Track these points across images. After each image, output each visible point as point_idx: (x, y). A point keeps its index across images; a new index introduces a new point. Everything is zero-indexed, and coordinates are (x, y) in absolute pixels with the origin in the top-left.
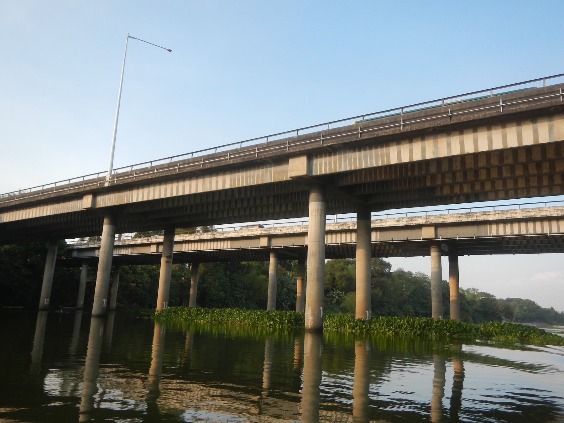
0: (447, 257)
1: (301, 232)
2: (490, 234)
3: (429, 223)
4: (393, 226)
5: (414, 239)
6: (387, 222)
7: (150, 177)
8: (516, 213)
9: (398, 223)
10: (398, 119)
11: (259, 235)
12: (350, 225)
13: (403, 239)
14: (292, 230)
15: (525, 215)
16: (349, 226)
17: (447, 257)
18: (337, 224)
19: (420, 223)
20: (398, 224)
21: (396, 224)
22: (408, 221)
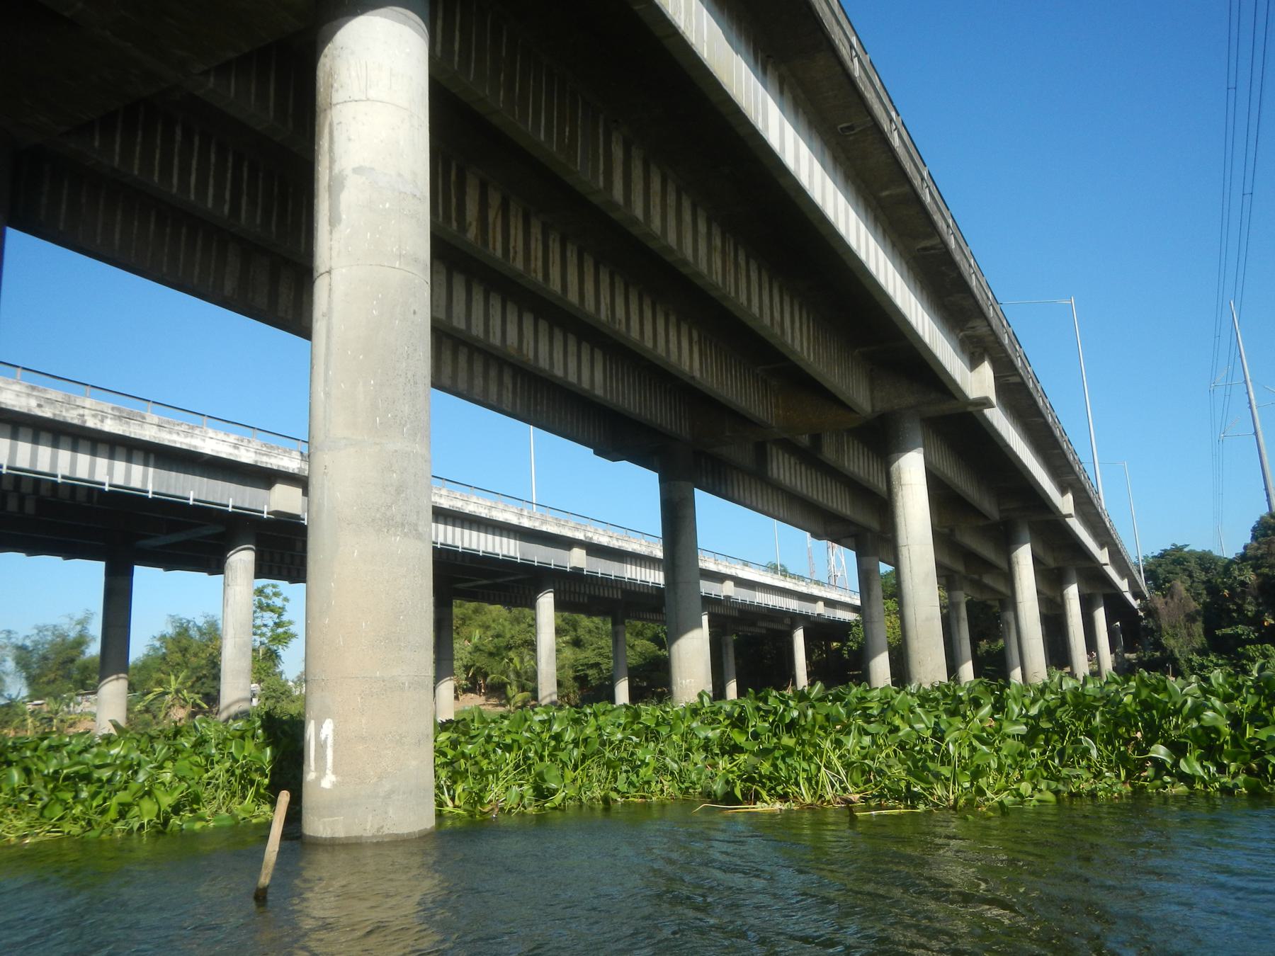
4: (224, 456)
5: (246, 506)
6: (207, 439)
8: (441, 496)
9: (236, 452)
12: (86, 412)
13: (218, 502)
15: (451, 503)
18: (35, 393)
19: (288, 468)
20: (236, 456)
21: (231, 454)
22: (260, 454)
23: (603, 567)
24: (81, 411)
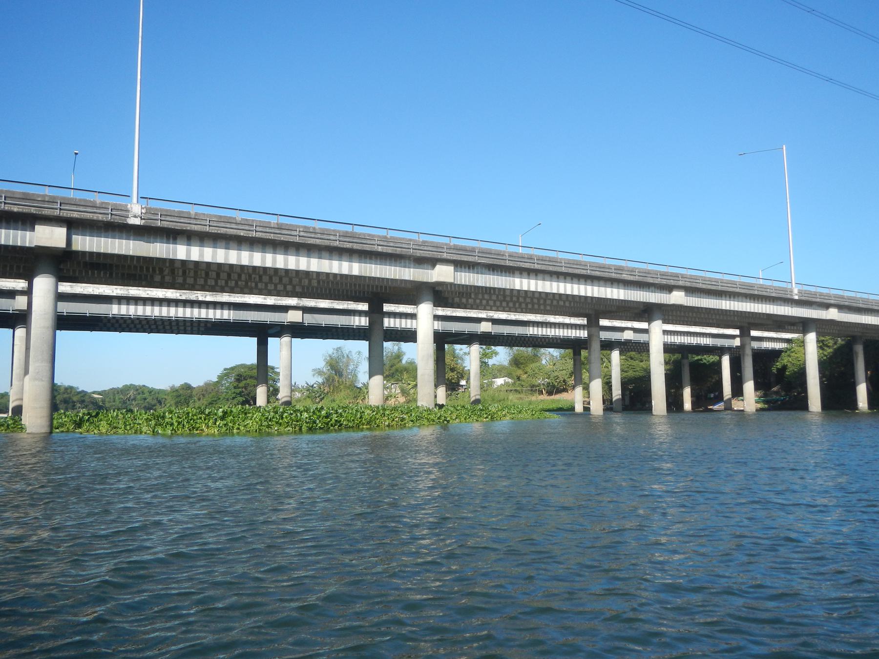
0: (255, 339)
1: (115, 295)
2: (354, 323)
3: (300, 305)
7: (242, 234)
9: (265, 301)
10: (533, 257)
11: (21, 289)
14: (95, 289)
16: (197, 295)
17: (255, 339)
23: (506, 330)
24: (197, 295)
